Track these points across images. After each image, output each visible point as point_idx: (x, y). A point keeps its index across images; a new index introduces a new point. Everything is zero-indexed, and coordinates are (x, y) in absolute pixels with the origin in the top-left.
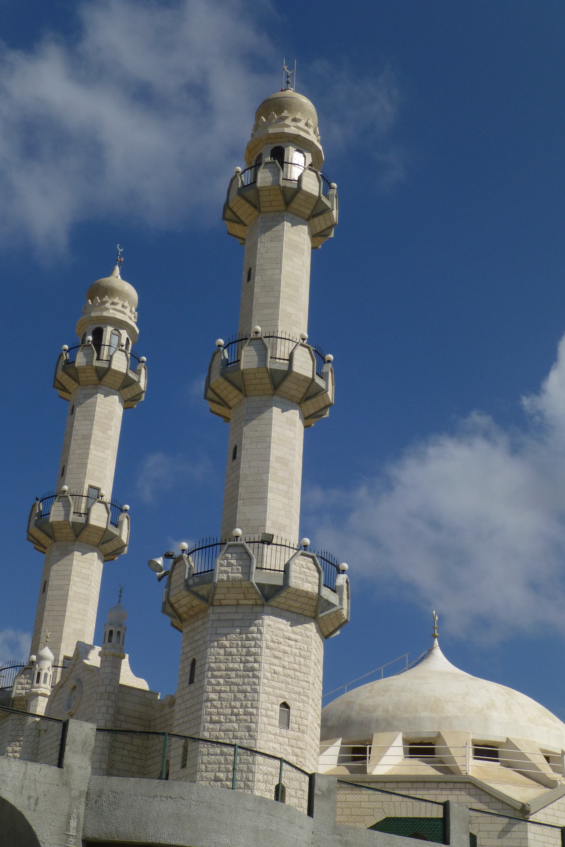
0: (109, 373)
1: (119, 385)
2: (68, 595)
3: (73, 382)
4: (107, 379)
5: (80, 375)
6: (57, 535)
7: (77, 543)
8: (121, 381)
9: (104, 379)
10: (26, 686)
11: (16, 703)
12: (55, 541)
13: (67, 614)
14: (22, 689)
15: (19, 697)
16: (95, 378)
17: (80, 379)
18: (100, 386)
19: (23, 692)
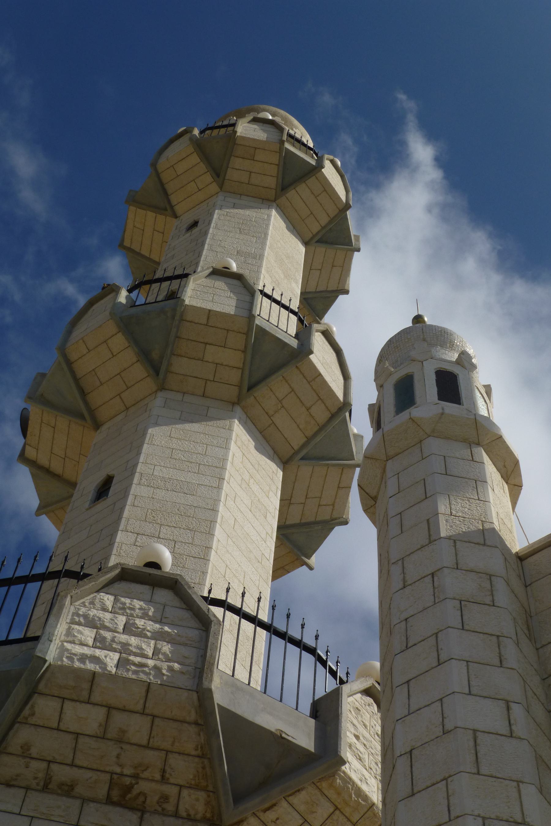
0: (312, 181)
1: (315, 228)
2: (214, 510)
3: (208, 178)
4: (299, 196)
5: (236, 162)
6: (180, 365)
7: (238, 409)
8: (324, 220)
9: (291, 194)
10: (124, 638)
11: (45, 708)
12: (162, 388)
13: (213, 556)
14: (100, 643)
15: (77, 674)
16: (271, 182)
17: (231, 174)
18: (275, 204)
19: (111, 660)
